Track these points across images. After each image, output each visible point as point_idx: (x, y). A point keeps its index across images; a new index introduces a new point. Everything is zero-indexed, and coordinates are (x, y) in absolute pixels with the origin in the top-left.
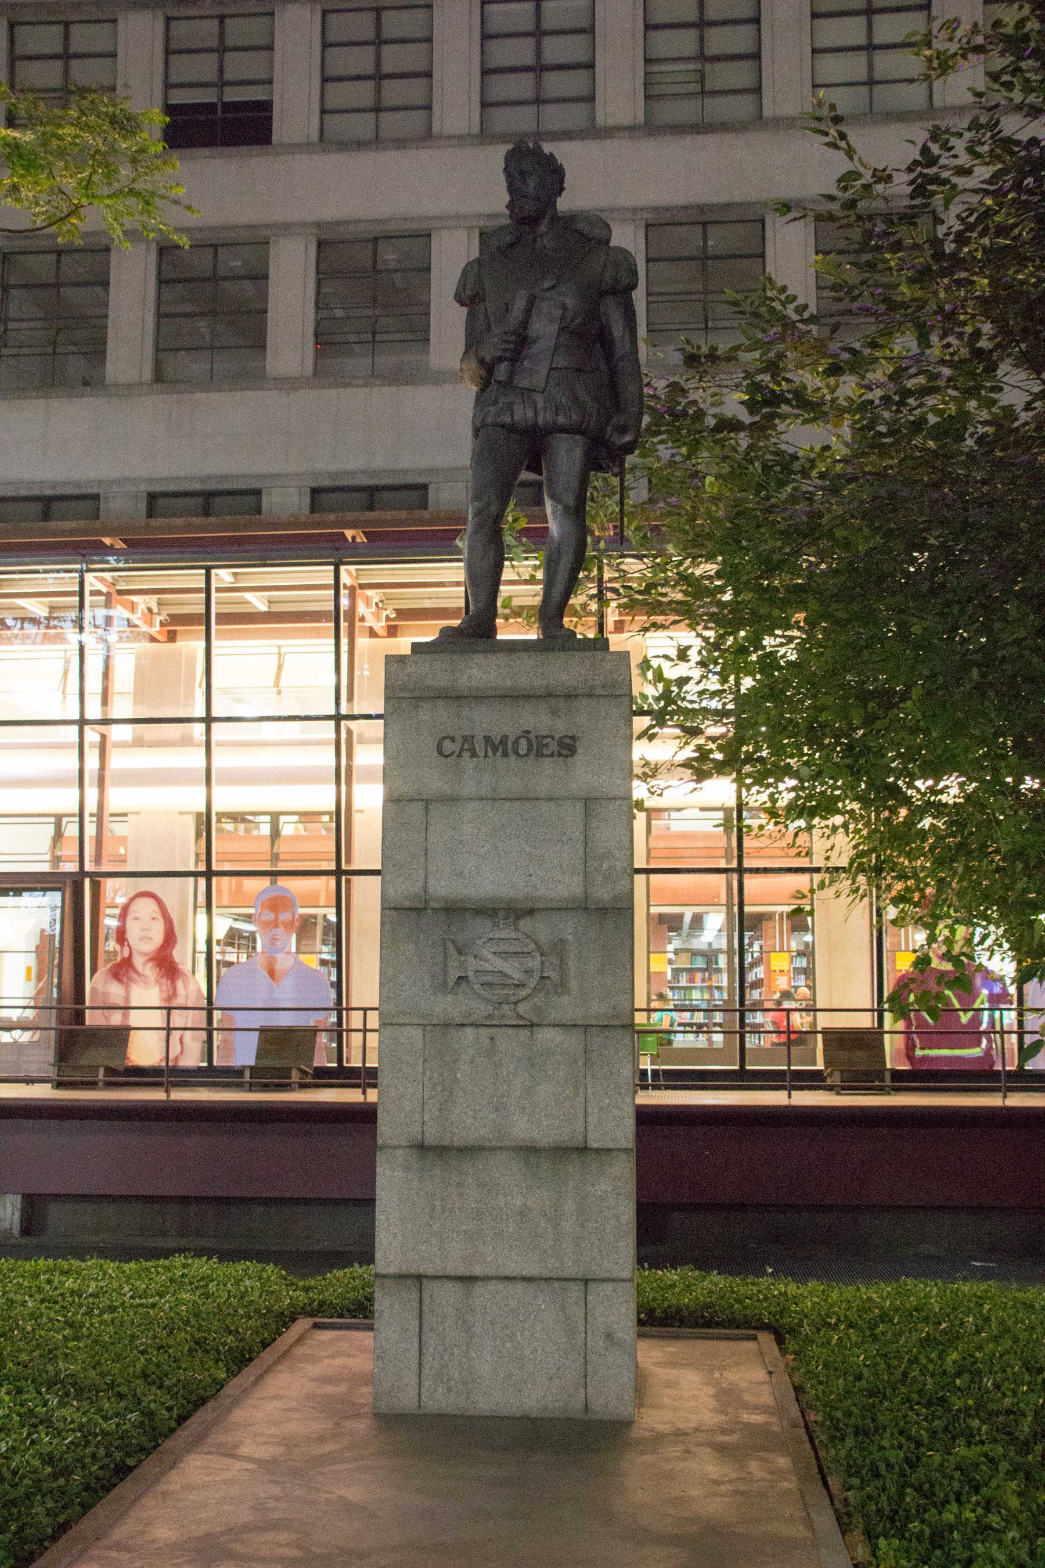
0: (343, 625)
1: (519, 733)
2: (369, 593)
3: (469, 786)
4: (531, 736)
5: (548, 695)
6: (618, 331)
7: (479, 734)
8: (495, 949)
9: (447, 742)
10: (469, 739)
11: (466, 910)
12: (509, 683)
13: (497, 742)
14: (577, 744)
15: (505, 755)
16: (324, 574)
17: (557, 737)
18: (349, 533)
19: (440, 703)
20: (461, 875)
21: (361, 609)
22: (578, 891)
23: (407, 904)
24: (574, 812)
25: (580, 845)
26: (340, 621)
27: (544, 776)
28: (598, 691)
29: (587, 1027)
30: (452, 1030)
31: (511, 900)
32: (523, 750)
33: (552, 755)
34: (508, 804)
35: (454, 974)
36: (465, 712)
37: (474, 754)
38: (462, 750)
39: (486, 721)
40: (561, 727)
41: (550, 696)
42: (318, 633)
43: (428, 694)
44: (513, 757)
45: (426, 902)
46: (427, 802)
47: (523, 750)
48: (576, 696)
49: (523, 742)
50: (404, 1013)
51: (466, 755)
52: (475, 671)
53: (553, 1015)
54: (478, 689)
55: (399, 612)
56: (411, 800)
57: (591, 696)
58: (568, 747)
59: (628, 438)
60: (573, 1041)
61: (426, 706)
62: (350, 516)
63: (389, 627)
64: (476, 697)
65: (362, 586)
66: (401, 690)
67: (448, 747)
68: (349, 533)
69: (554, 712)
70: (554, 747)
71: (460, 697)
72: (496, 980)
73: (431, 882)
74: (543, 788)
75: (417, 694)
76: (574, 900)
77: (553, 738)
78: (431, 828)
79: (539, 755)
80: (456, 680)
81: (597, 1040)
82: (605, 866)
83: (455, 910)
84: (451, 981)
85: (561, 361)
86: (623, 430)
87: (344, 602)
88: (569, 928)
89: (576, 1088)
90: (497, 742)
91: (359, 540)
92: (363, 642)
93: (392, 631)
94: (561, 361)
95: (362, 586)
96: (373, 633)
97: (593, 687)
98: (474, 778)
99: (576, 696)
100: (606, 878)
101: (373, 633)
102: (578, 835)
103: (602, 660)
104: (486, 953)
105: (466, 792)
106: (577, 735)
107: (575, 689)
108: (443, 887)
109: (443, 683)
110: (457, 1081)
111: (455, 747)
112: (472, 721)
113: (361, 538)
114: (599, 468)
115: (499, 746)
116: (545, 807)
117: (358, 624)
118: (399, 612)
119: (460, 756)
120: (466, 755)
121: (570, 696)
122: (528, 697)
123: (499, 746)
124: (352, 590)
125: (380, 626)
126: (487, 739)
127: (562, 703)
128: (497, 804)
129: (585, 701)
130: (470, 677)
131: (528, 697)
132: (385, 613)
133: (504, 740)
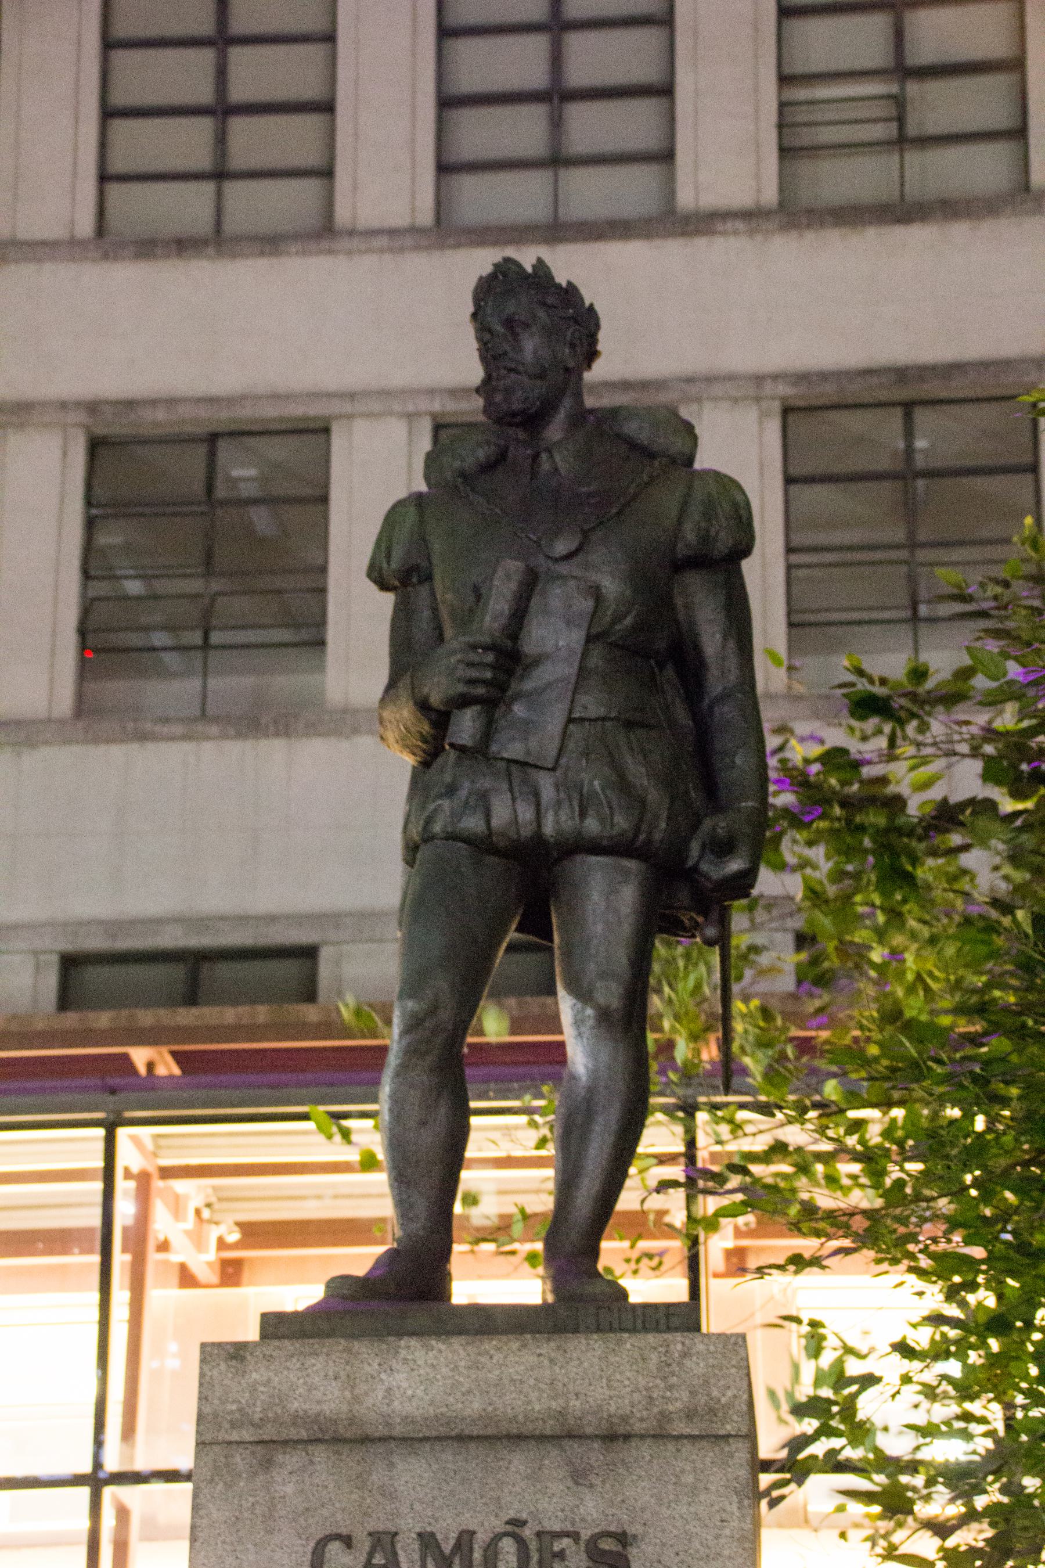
0: (120, 1259)
1: (499, 1526)
2: (181, 1186)
4: (527, 1532)
6: (712, 640)
7: (409, 1527)
12: (476, 1405)
13: (447, 1548)
14: (633, 1552)
16: (82, 1146)
17: (585, 1534)
18: (140, 1056)
19: (320, 1454)
21: (163, 1223)
26: (111, 1247)
28: (681, 1427)
41: (570, 1436)
42: (61, 1279)
43: (293, 1433)
48: (627, 1437)
49: (508, 1545)
52: (400, 1379)
54: (407, 1420)
55: (242, 1226)
57: (660, 1436)
59: (735, 865)
61: (291, 1460)
62: (146, 1017)
63: (225, 1263)
64: (406, 1440)
65: (166, 1173)
66: (234, 1425)
68: (140, 1056)
69: (579, 1476)
71: (366, 1440)
75: (269, 1432)
77: (575, 1536)
80: (357, 1399)
85: (592, 705)
86: (724, 848)
87: (125, 1209)
90: (447, 1548)
91: (161, 1071)
92: (163, 1298)
93: (231, 1272)
94: (592, 705)
95: (166, 1173)
96: (187, 1278)
97: (665, 1417)
99: (627, 1437)
101: (187, 1278)
103: (685, 1355)
106: (631, 1530)
107: (625, 1419)
109: (327, 1408)
112: (392, 1496)
113: (168, 1067)
114: (674, 927)
117: (153, 1257)
118: (242, 1226)
121: (615, 1436)
122: (517, 1439)
124: (143, 1180)
125: (203, 1261)
126: (427, 1541)
127: (595, 1454)
129: (645, 1450)
130: (389, 1390)
131: (517, 1439)
132: (214, 1233)
133: (466, 1538)
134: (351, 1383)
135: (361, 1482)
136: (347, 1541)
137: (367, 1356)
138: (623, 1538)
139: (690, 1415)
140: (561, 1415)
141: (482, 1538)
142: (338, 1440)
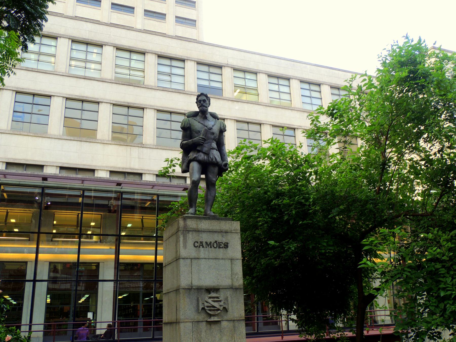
3: (202, 255)
5: (221, 232)
7: (204, 241)
8: (213, 300)
9: (196, 243)
10: (201, 242)
11: (202, 289)
12: (211, 228)
15: (211, 247)
19: (194, 232)
20: (201, 279)
22: (230, 283)
23: (187, 287)
24: (228, 263)
25: (230, 271)
27: (221, 253)
29: (234, 320)
30: (200, 323)
31: (214, 286)
32: (215, 246)
33: (222, 248)
34: (212, 260)
35: (201, 306)
36: (201, 235)
37: (203, 247)
38: (200, 245)
39: (205, 238)
40: (224, 240)
44: (213, 248)
45: (192, 287)
46: (191, 259)
47: (215, 246)
49: (215, 244)
50: (187, 319)
51: (201, 247)
53: (225, 318)
56: (187, 259)
57: (231, 232)
58: (226, 246)
60: (231, 324)
67: (196, 244)
69: (222, 236)
70: (223, 245)
72: (212, 309)
73: (193, 281)
74: (221, 256)
76: (229, 286)
78: (193, 266)
79: (219, 248)
81: (236, 324)
82: (236, 277)
83: (199, 289)
84: (200, 309)
88: (229, 293)
89: (232, 337)
97: (231, 230)
98: (203, 252)
100: (237, 280)
102: (230, 269)
104: (210, 301)
105: (201, 257)
108: (196, 283)
110: (201, 337)
111: (198, 244)
115: (209, 245)
116: (221, 261)
119: (199, 247)
120: (201, 247)
121: (226, 232)
122: (216, 232)
123: (209, 245)
126: (206, 243)
127: (224, 234)
128: (210, 260)
129: (230, 234)
131: (216, 232)
133: (210, 243)
134: (197, 224)
135: (199, 236)
136: (197, 242)
137: (199, 222)
138: (227, 243)
139: (234, 230)
140: (221, 230)
141: (213, 242)
142: (195, 231)
